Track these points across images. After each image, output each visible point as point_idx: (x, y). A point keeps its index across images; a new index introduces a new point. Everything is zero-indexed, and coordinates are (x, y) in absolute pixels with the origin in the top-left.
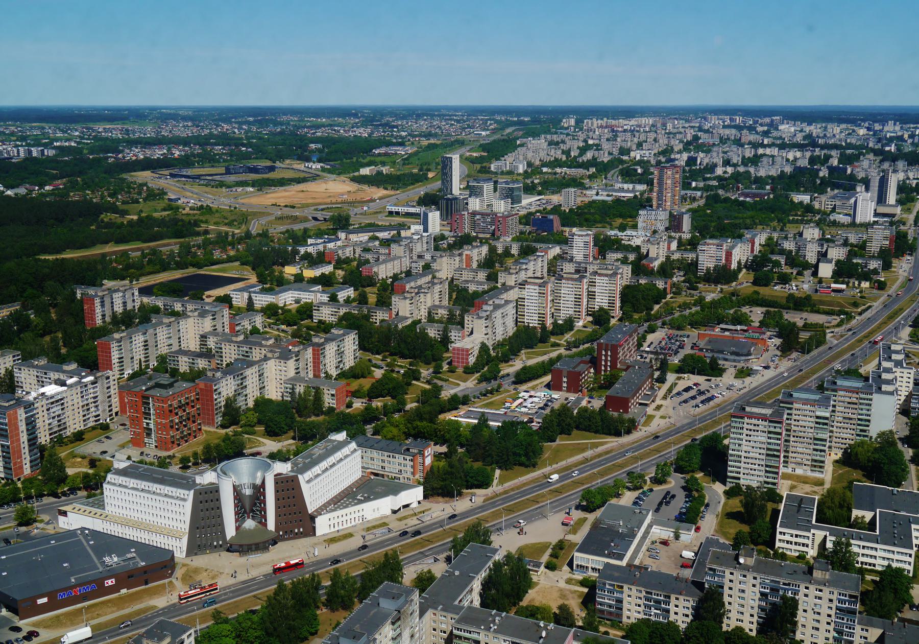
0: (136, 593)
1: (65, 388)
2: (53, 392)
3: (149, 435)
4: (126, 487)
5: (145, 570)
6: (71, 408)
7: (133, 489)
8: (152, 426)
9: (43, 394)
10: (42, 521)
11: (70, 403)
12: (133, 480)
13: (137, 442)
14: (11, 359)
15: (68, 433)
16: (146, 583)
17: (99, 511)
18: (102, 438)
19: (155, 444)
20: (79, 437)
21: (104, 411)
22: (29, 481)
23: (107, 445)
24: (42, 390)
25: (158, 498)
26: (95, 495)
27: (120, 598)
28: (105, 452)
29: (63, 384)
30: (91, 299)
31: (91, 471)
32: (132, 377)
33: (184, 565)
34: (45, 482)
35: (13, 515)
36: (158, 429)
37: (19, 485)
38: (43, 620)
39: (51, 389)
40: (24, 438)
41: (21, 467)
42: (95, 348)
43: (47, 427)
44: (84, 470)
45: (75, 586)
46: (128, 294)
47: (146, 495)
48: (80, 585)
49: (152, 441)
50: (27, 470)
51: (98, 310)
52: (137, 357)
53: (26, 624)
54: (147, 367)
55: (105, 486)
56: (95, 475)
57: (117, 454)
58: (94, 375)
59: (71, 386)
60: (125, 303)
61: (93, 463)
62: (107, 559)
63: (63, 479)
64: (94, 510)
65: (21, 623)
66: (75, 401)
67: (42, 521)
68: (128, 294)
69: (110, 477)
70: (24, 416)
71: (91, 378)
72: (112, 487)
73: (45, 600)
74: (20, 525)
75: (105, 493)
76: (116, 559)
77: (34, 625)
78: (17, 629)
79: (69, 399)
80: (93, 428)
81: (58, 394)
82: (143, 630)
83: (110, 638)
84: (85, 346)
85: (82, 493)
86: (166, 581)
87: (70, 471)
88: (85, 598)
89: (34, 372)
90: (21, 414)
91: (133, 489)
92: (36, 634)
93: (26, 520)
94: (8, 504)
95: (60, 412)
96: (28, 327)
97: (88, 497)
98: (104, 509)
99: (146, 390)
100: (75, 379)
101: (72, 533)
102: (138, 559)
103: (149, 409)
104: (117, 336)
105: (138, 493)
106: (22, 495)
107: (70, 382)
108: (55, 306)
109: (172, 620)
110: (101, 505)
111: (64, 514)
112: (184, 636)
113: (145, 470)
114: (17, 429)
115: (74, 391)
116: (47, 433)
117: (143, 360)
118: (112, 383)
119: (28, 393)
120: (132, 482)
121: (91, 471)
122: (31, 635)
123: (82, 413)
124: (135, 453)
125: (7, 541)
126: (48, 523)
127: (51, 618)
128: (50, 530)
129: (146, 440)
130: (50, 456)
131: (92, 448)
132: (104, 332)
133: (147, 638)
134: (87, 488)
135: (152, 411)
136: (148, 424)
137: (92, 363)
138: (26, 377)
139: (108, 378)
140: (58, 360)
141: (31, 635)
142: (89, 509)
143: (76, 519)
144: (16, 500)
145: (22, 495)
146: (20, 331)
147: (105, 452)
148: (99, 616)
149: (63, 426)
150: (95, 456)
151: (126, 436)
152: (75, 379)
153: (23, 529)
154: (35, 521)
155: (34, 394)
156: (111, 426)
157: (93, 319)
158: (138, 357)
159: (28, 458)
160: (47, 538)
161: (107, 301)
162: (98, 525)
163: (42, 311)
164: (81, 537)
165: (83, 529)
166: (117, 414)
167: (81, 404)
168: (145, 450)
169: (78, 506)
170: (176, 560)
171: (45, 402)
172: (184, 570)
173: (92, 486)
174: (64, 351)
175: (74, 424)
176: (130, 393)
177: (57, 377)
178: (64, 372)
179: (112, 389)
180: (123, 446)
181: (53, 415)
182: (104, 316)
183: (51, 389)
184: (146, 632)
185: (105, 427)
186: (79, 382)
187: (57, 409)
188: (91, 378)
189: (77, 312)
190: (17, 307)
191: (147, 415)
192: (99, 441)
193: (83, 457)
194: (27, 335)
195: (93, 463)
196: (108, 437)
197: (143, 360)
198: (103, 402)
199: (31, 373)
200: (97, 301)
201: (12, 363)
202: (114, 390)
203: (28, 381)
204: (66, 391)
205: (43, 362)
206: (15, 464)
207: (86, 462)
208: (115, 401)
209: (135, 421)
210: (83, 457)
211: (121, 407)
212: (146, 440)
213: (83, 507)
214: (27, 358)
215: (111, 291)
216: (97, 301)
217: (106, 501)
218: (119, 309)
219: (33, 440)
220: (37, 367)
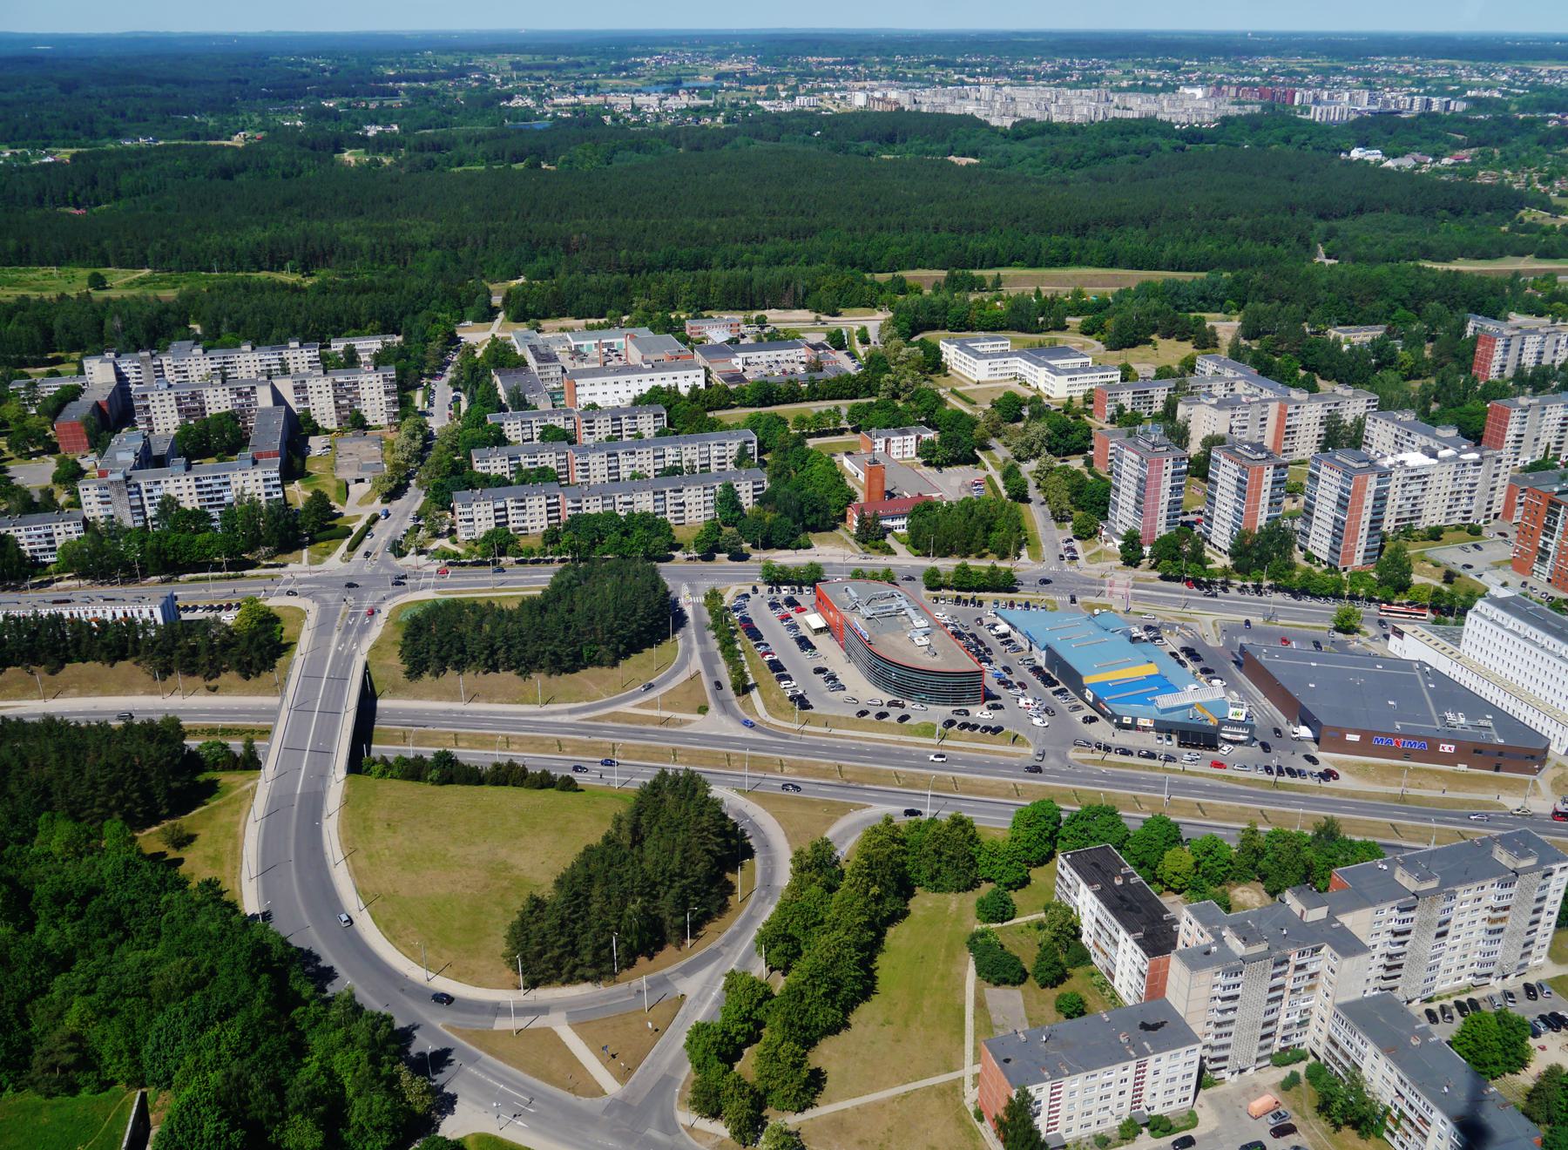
0: (1479, 776)
1: (1434, 461)
2: (1417, 464)
3: (1542, 560)
4: (1500, 625)
5: (1501, 751)
6: (1434, 491)
7: (1511, 631)
8: (1551, 549)
9: (1402, 463)
10: (1365, 634)
11: (1436, 484)
12: (1514, 620)
13: (1520, 565)
14: (1365, 404)
15: (1422, 525)
16: (1497, 769)
17: (1450, 647)
18: (1469, 545)
19: (1547, 575)
20: (1435, 534)
21: (1480, 507)
22: (1359, 576)
23: (1472, 557)
24: (1401, 457)
25: (1547, 657)
26: (1445, 623)
27: (1455, 775)
28: (1469, 567)
29: (1434, 455)
30: (1491, 340)
31: (1446, 588)
32: (1534, 467)
33: (1559, 765)
34: (1382, 583)
35: (1334, 615)
36: (1560, 556)
37: (1344, 575)
38: (1347, 762)
39: (1415, 459)
40: (1367, 516)
41: (1352, 555)
42: (1485, 413)
43: (1396, 509)
44: (1438, 584)
45: (1399, 735)
46: (1550, 341)
47: (1530, 647)
48: (1406, 737)
49: (1546, 570)
50: (1358, 561)
51: (1497, 357)
52: (1544, 440)
53: (1327, 759)
54: (1556, 458)
55: (1469, 614)
56: (1452, 596)
57: (1486, 574)
58: (1480, 452)
59: (1443, 460)
60: (1540, 353)
61: (1449, 577)
62: (1450, 716)
63: (1403, 587)
64: (1443, 643)
65: (1319, 755)
66: (1444, 483)
67: (1365, 634)
68: (1550, 341)
69: (1480, 604)
70: (1375, 486)
71: (1475, 456)
72: (1480, 620)
73: (1356, 738)
74: (1338, 629)
75: (1468, 624)
76: (1463, 720)
77: (1334, 763)
78: (1312, 760)
79: (1435, 478)
80: (1458, 528)
81: (1423, 467)
82: (1497, 833)
83: (1437, 821)
84: (1469, 406)
85: (1429, 614)
86: (1532, 777)
87: (1416, 579)
88: (1407, 755)
89: (1393, 429)
90: (1372, 483)
91: (1511, 631)
92: (1337, 778)
93: (1346, 627)
94: (1326, 597)
95: (1419, 493)
96: (1391, 362)
97: (1436, 622)
98: (1458, 646)
99: (1560, 493)
100: (1450, 452)
101: (1408, 664)
102: (1494, 732)
103: (1556, 523)
104: (1523, 401)
105: (1518, 641)
106: (1346, 593)
107: (1442, 454)
108: (1432, 339)
109: (1542, 837)
110: (1456, 640)
111: (1400, 634)
112: (1557, 867)
113: (1535, 610)
114: (1362, 502)
115: (1446, 469)
116: (1394, 517)
117: (1553, 445)
118: (1503, 469)
119: (1383, 456)
120: (1513, 622)
121: (1446, 588)
122: (1328, 775)
123: (1447, 503)
124: (1515, 579)
125: (1317, 645)
126: (1373, 639)
127: (1357, 765)
128: (1376, 648)
129: (1536, 566)
130: (1398, 550)
131: (1451, 554)
132: (1496, 391)
133: (1503, 847)
134: (1435, 609)
135: (1559, 527)
136: (1546, 544)
137: (1474, 435)
138: (1380, 433)
139: (1499, 461)
140: (1431, 420)
141: (1328, 775)
142: (1436, 639)
143: (1415, 645)
144: (1338, 596)
145: (1346, 593)
146: (1379, 366)
147: (1469, 567)
148: (1420, 786)
149: (1416, 514)
150: (1453, 568)
151: (1508, 552)
152: (1450, 452)
153: (1340, 636)
154: (1358, 631)
155: (1390, 461)
156: (1485, 532)
157: (1485, 368)
158: (1547, 440)
159: (1364, 545)
160: (1374, 659)
161: (1515, 344)
162: (1444, 665)
163: (1414, 342)
164: (1418, 673)
165: (1423, 664)
166: (1496, 516)
167: (1450, 489)
168: (1531, 581)
169: (1422, 630)
170: (1550, 754)
171: (1402, 474)
172: (1558, 772)
173: (1449, 607)
174: (1434, 407)
175: (1433, 515)
176: (1532, 491)
177: (1424, 443)
178: (1436, 438)
179: (1499, 479)
180: (1497, 566)
181: (1407, 494)
182: (1503, 366)
183: (1415, 459)
184: (1501, 837)
185: (1475, 531)
186: (1455, 458)
187: (1415, 488)
188: (1475, 456)
189: (1464, 355)
190: (1378, 332)
191: (1549, 530)
192: (1463, 548)
193: (1436, 565)
194: (1390, 375)
195: (1449, 577)
196: (1476, 546)
197: (1553, 445)
198: (1483, 494)
199: (1389, 429)
200: (1500, 343)
201: (1364, 410)
202: (1502, 482)
203: (1382, 439)
204: (1434, 466)
205: (1409, 416)
206: (1346, 547)
207: (1440, 573)
208: (1500, 498)
209: (1524, 532)
210: (1436, 565)
211: (1506, 508)
212: (1536, 566)
213: (1429, 635)
214: (1385, 406)
215: (1527, 332)
216: (1500, 343)
217: (1465, 636)
218: (1529, 361)
219: (1376, 523)
220: (1399, 422)
